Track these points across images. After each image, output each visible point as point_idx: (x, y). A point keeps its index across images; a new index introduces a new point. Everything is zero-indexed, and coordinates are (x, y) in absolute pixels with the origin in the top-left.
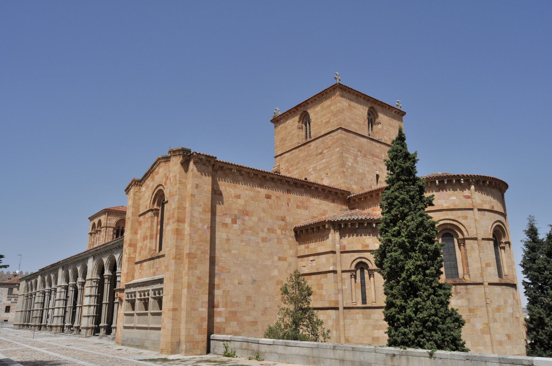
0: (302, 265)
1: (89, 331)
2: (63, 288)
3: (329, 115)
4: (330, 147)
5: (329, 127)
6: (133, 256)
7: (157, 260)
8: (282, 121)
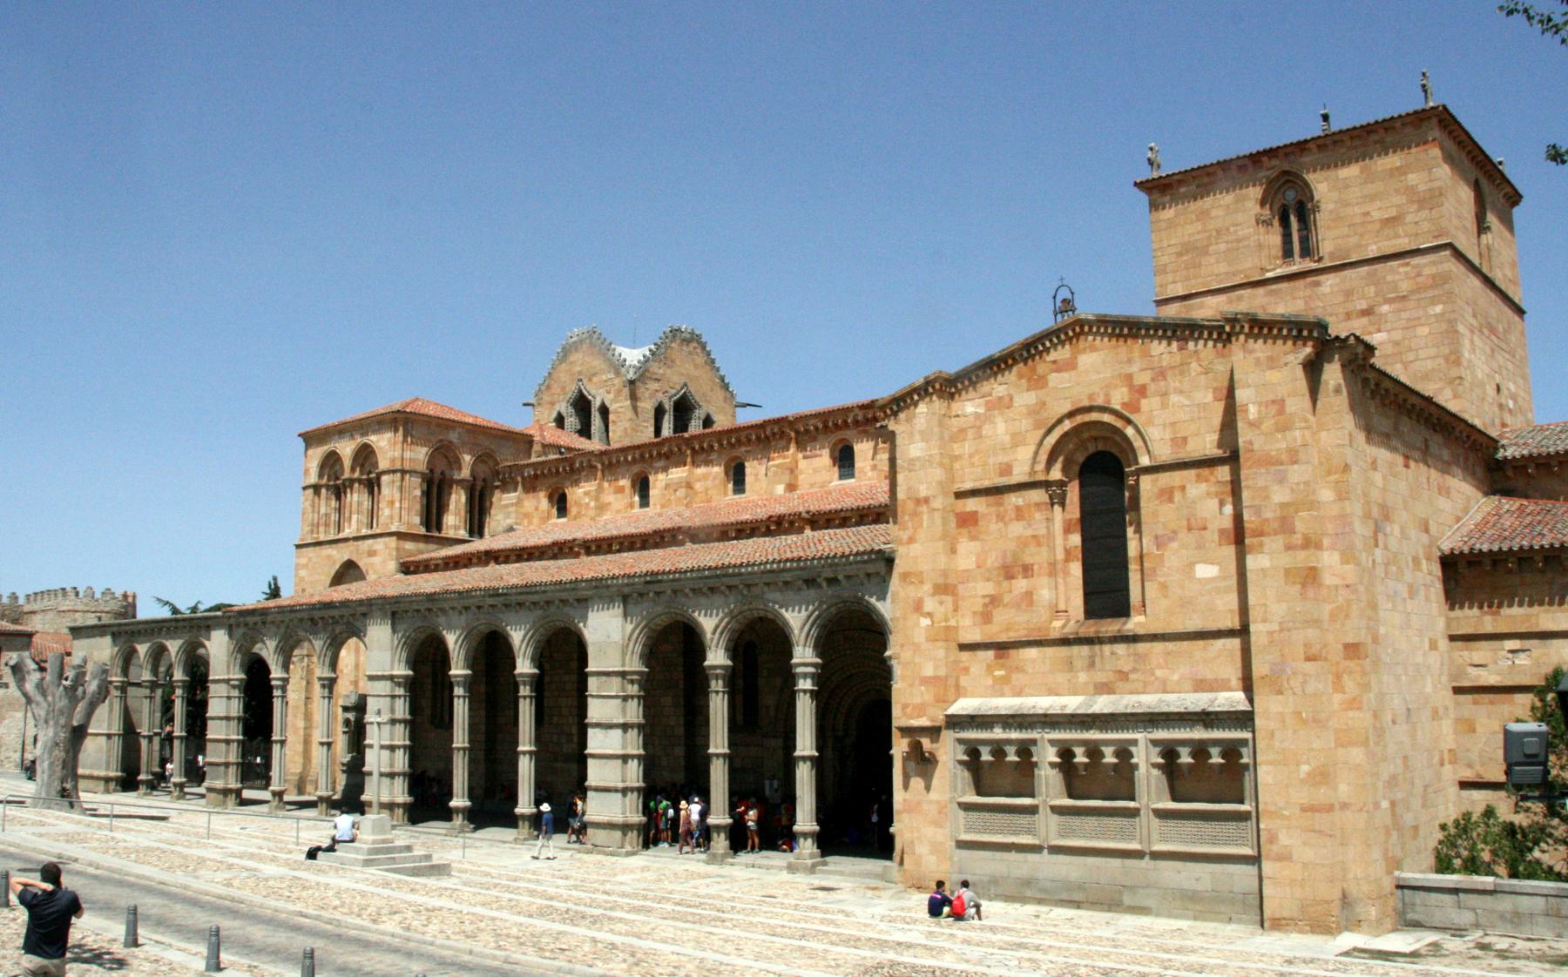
0: (1469, 661)
1: (633, 835)
2: (399, 684)
3: (1399, 200)
4: (1404, 297)
5: (1397, 236)
6: (952, 623)
7: (1121, 649)
8: (1183, 190)
